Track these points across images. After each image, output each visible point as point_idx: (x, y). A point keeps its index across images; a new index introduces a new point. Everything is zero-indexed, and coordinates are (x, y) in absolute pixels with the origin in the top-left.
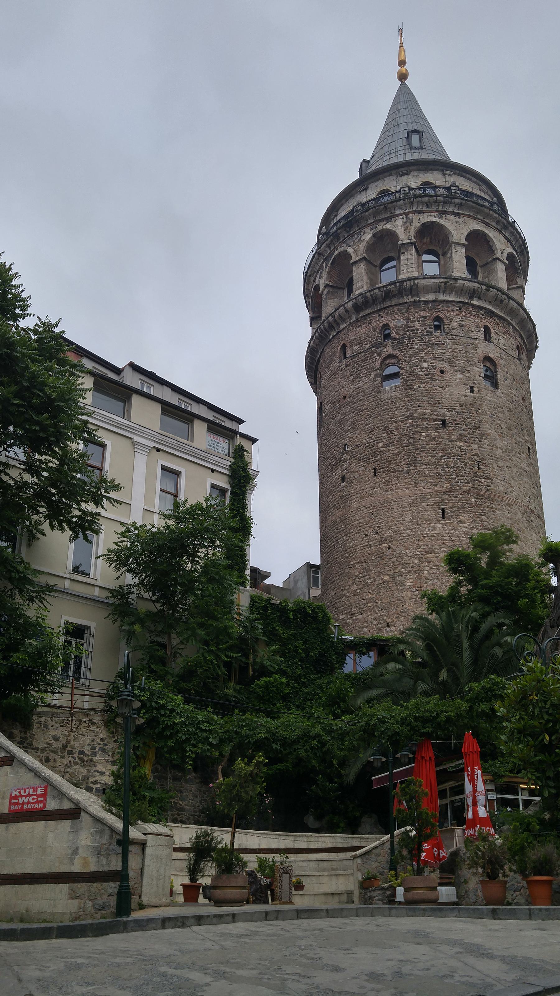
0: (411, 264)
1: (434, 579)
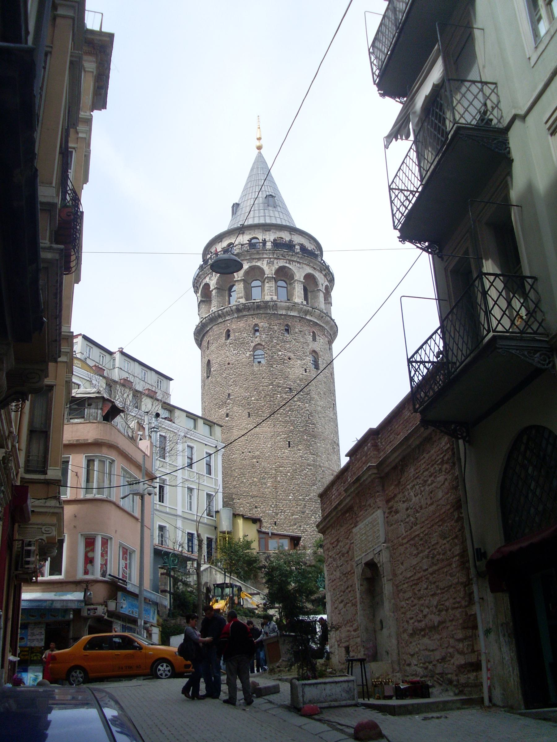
0: (273, 290)
1: (283, 482)
